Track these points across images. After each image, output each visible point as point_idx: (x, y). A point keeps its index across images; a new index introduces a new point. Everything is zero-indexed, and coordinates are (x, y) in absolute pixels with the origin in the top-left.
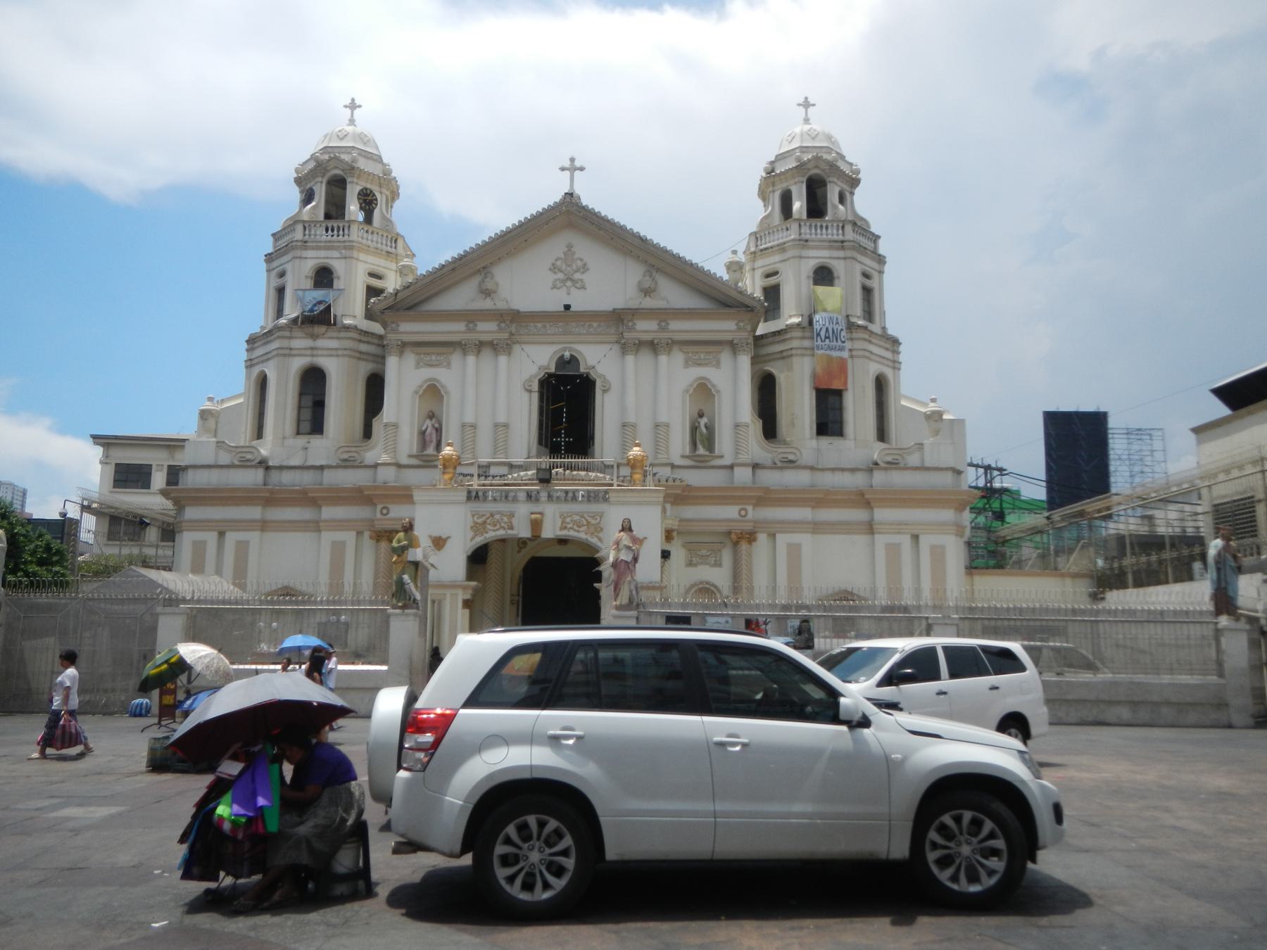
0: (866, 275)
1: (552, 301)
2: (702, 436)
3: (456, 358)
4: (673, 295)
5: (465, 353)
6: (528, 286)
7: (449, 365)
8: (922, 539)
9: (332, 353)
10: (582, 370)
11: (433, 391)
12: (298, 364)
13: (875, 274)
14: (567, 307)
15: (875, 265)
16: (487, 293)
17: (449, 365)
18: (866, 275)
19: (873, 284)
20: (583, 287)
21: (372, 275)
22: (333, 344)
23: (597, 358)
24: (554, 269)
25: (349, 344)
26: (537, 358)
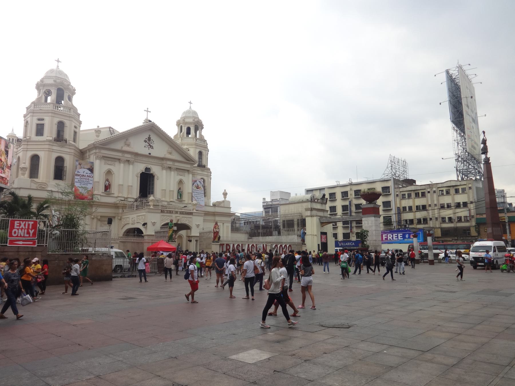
0: (75, 127)
1: (145, 151)
2: (180, 194)
3: (117, 163)
4: (175, 156)
5: (189, 173)
6: (139, 146)
7: (114, 165)
8: (225, 224)
9: (67, 153)
10: (151, 172)
11: (109, 172)
12: (55, 155)
13: (78, 127)
14: (150, 154)
15: (78, 124)
16: (128, 145)
17: (114, 165)
18: (75, 127)
19: (77, 130)
20: (152, 148)
21: (39, 120)
22: (68, 150)
23: (155, 170)
24: (145, 141)
25: (47, 147)
26: (141, 168)
